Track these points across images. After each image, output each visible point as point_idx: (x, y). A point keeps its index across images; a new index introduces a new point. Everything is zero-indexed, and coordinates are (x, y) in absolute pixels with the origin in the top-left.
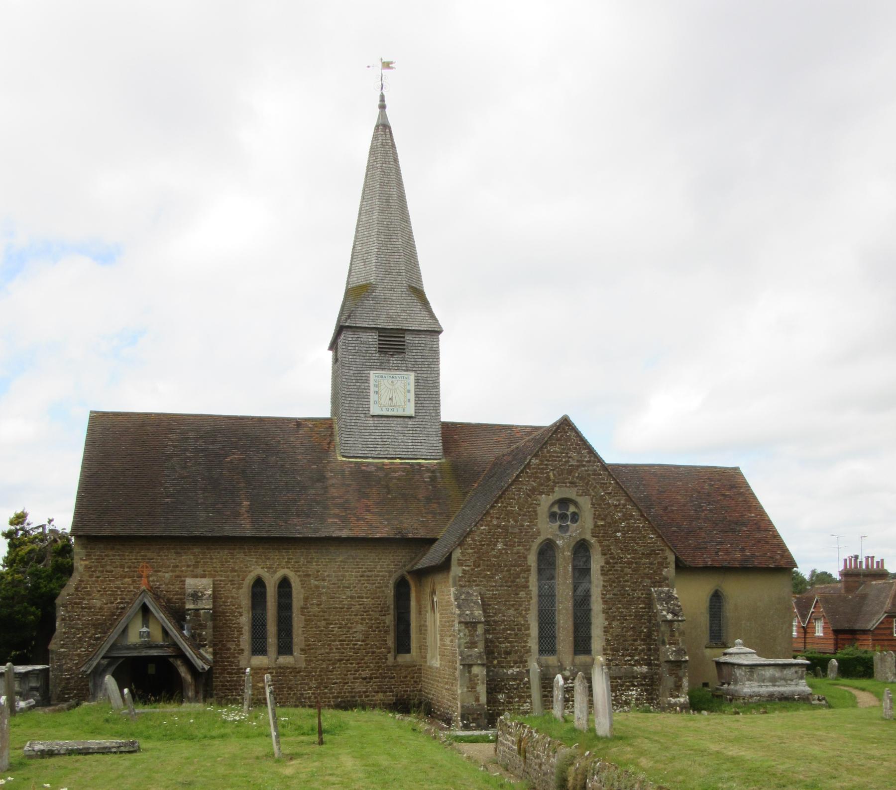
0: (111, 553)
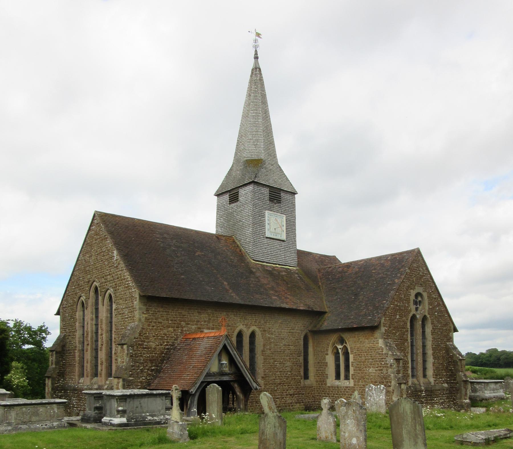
0: (161, 310)
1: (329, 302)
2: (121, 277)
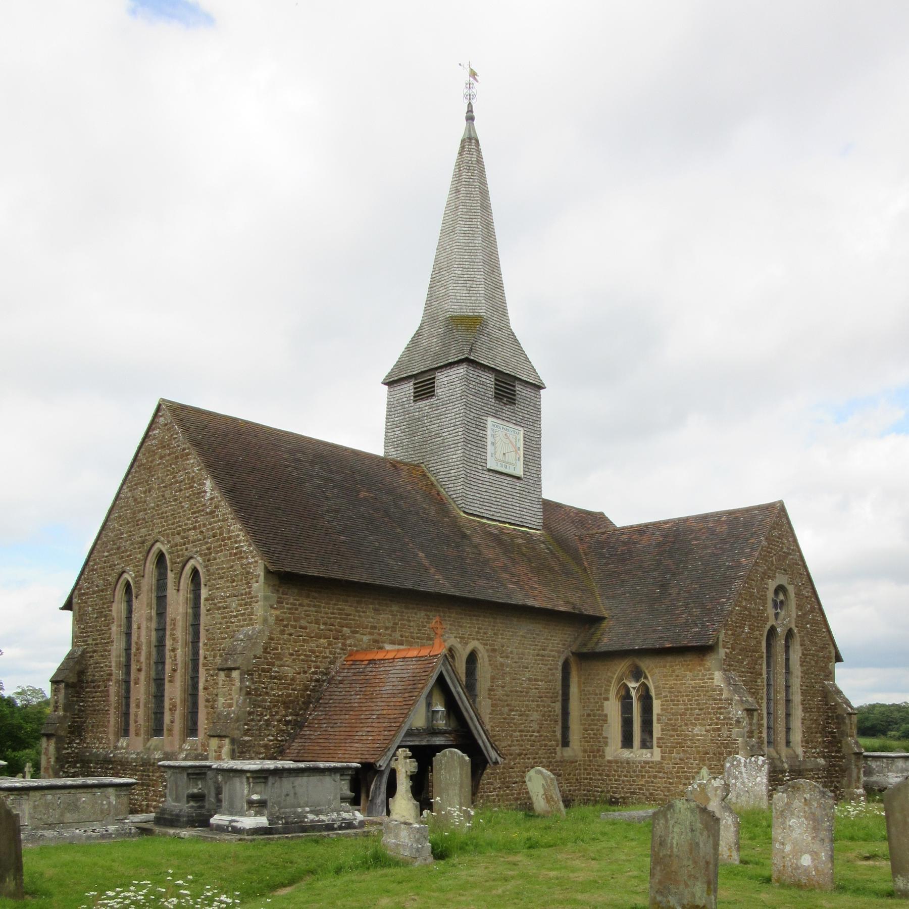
0: (306, 601)
1: (607, 598)
2: (221, 534)
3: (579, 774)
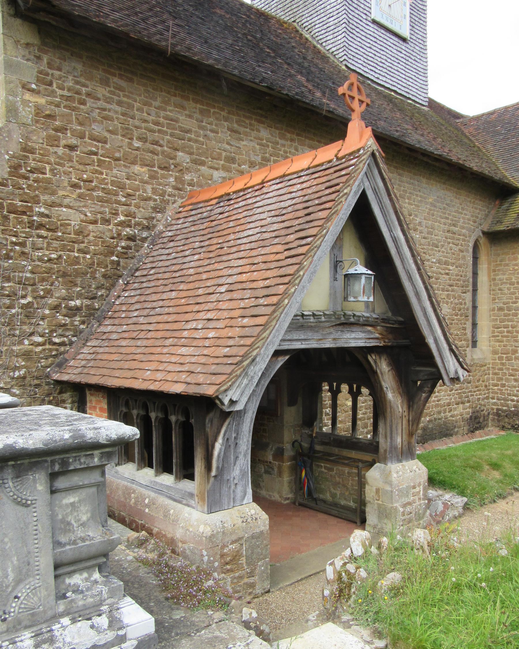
0: (102, 91)
3: (488, 379)
